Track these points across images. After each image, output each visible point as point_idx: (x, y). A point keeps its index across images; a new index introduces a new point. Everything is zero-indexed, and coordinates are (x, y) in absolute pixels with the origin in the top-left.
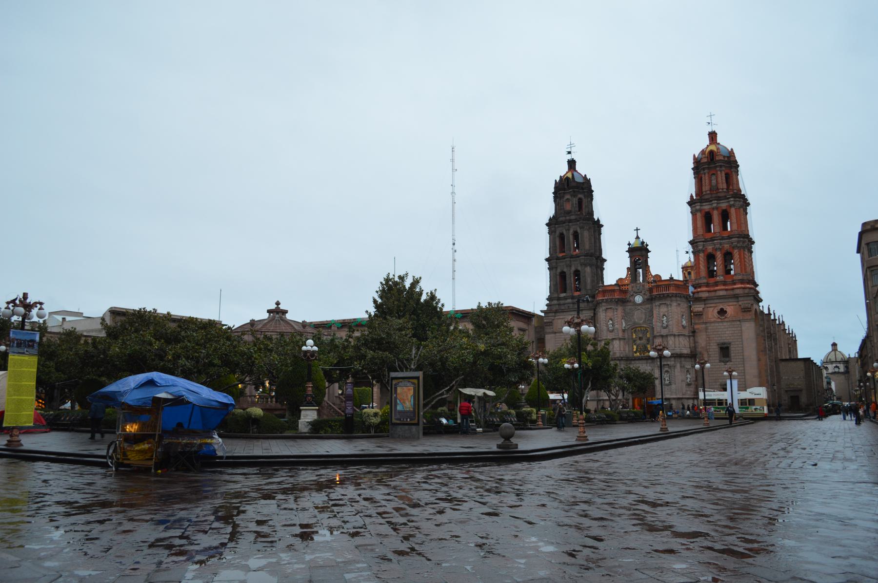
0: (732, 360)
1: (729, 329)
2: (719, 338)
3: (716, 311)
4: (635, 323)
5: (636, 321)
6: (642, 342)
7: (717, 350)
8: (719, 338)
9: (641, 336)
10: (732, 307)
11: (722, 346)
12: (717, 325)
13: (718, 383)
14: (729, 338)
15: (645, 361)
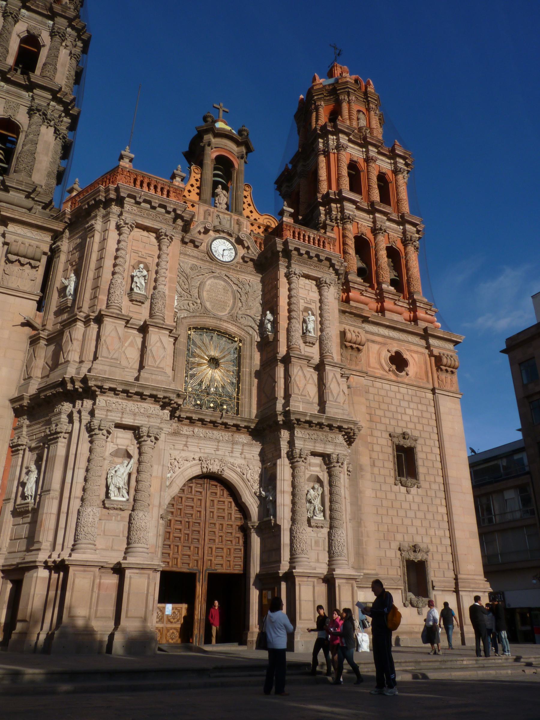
0: (422, 483)
1: (412, 405)
2: (393, 422)
3: (385, 355)
4: (206, 312)
5: (208, 305)
6: (217, 374)
7: (390, 450)
8: (393, 422)
9: (214, 353)
10: (415, 356)
11: (402, 442)
12: (387, 387)
13: (395, 545)
14: (411, 426)
15: (226, 435)
